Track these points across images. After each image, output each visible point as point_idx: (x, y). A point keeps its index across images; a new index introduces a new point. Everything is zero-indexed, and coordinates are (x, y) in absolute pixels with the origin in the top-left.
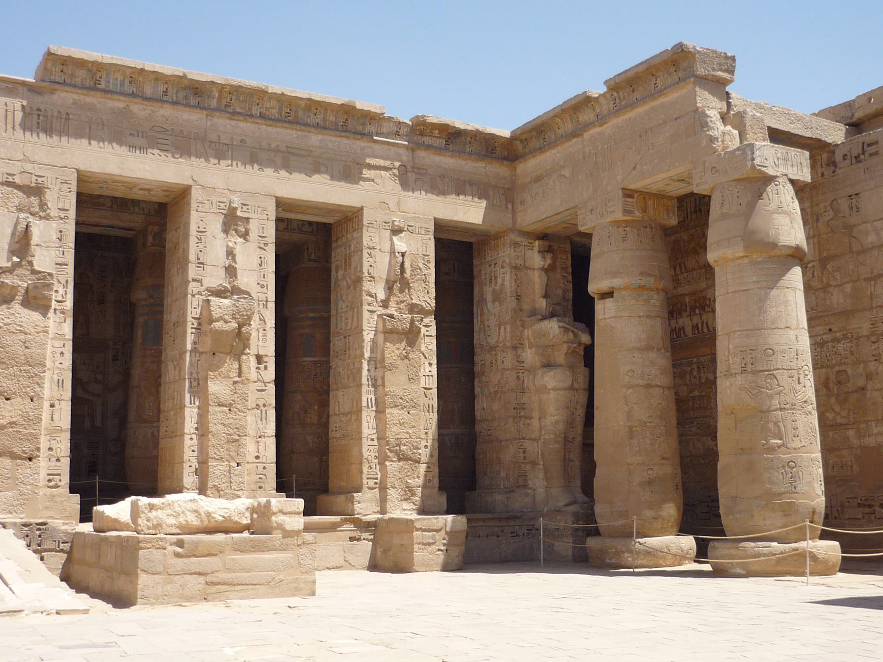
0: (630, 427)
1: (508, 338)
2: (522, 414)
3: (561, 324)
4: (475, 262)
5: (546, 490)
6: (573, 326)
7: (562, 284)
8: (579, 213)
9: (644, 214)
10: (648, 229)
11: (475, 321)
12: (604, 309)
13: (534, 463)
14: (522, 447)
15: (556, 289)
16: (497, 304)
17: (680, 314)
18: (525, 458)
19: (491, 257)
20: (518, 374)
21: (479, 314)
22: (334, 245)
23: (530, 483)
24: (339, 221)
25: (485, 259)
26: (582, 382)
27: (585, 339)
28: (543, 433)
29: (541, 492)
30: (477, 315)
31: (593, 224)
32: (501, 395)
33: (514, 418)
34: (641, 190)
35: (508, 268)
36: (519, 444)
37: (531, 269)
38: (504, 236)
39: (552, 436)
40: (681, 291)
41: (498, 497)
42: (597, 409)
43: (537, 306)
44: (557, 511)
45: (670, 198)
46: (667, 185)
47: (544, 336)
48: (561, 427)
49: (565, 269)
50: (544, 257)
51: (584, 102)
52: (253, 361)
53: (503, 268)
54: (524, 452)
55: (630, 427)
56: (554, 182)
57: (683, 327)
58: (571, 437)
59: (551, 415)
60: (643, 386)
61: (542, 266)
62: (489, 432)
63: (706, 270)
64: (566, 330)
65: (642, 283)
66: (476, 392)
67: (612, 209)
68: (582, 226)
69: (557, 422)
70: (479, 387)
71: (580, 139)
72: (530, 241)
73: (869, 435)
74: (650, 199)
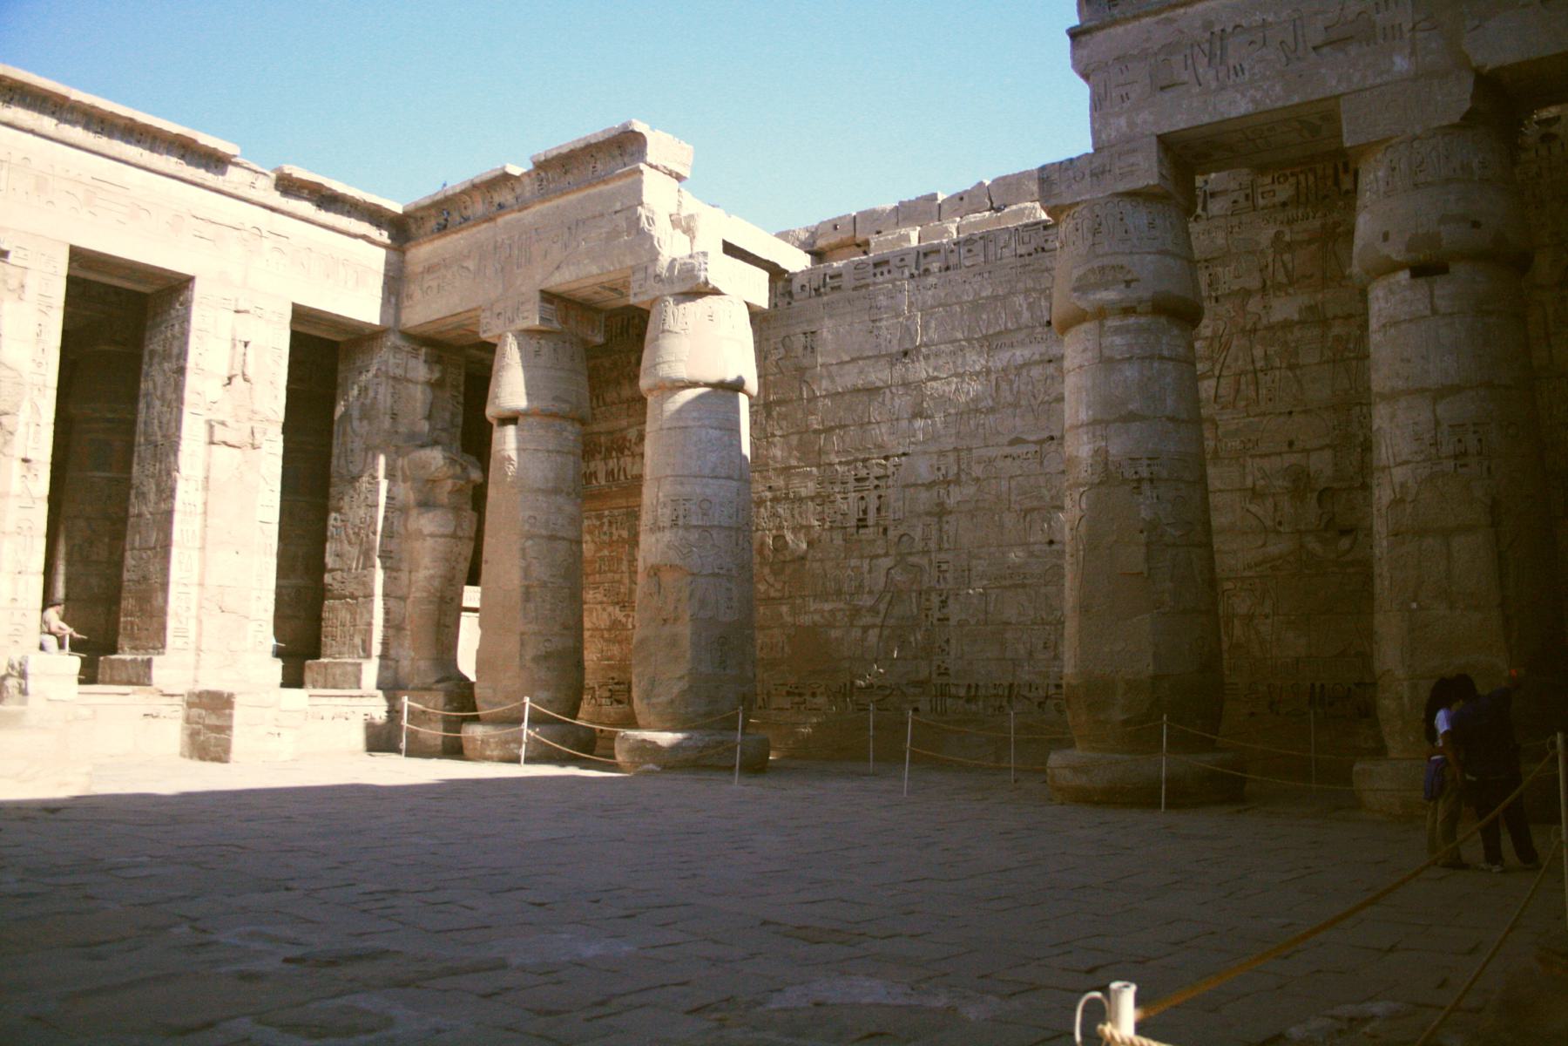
0: (527, 587)
3: (447, 454)
4: (341, 367)
8: (483, 315)
10: (567, 345)
11: (335, 442)
16: (365, 423)
17: (593, 456)
22: (149, 323)
24: (158, 292)
25: (354, 364)
26: (468, 529)
27: (476, 475)
34: (565, 295)
37: (412, 381)
39: (425, 594)
40: (596, 428)
45: (598, 311)
46: (596, 293)
48: (437, 583)
50: (431, 370)
51: (505, 179)
52: (17, 466)
57: (595, 472)
64: (452, 462)
65: (555, 409)
66: (329, 534)
67: (526, 314)
68: (485, 332)
69: (432, 577)
71: (491, 224)
73: (805, 613)
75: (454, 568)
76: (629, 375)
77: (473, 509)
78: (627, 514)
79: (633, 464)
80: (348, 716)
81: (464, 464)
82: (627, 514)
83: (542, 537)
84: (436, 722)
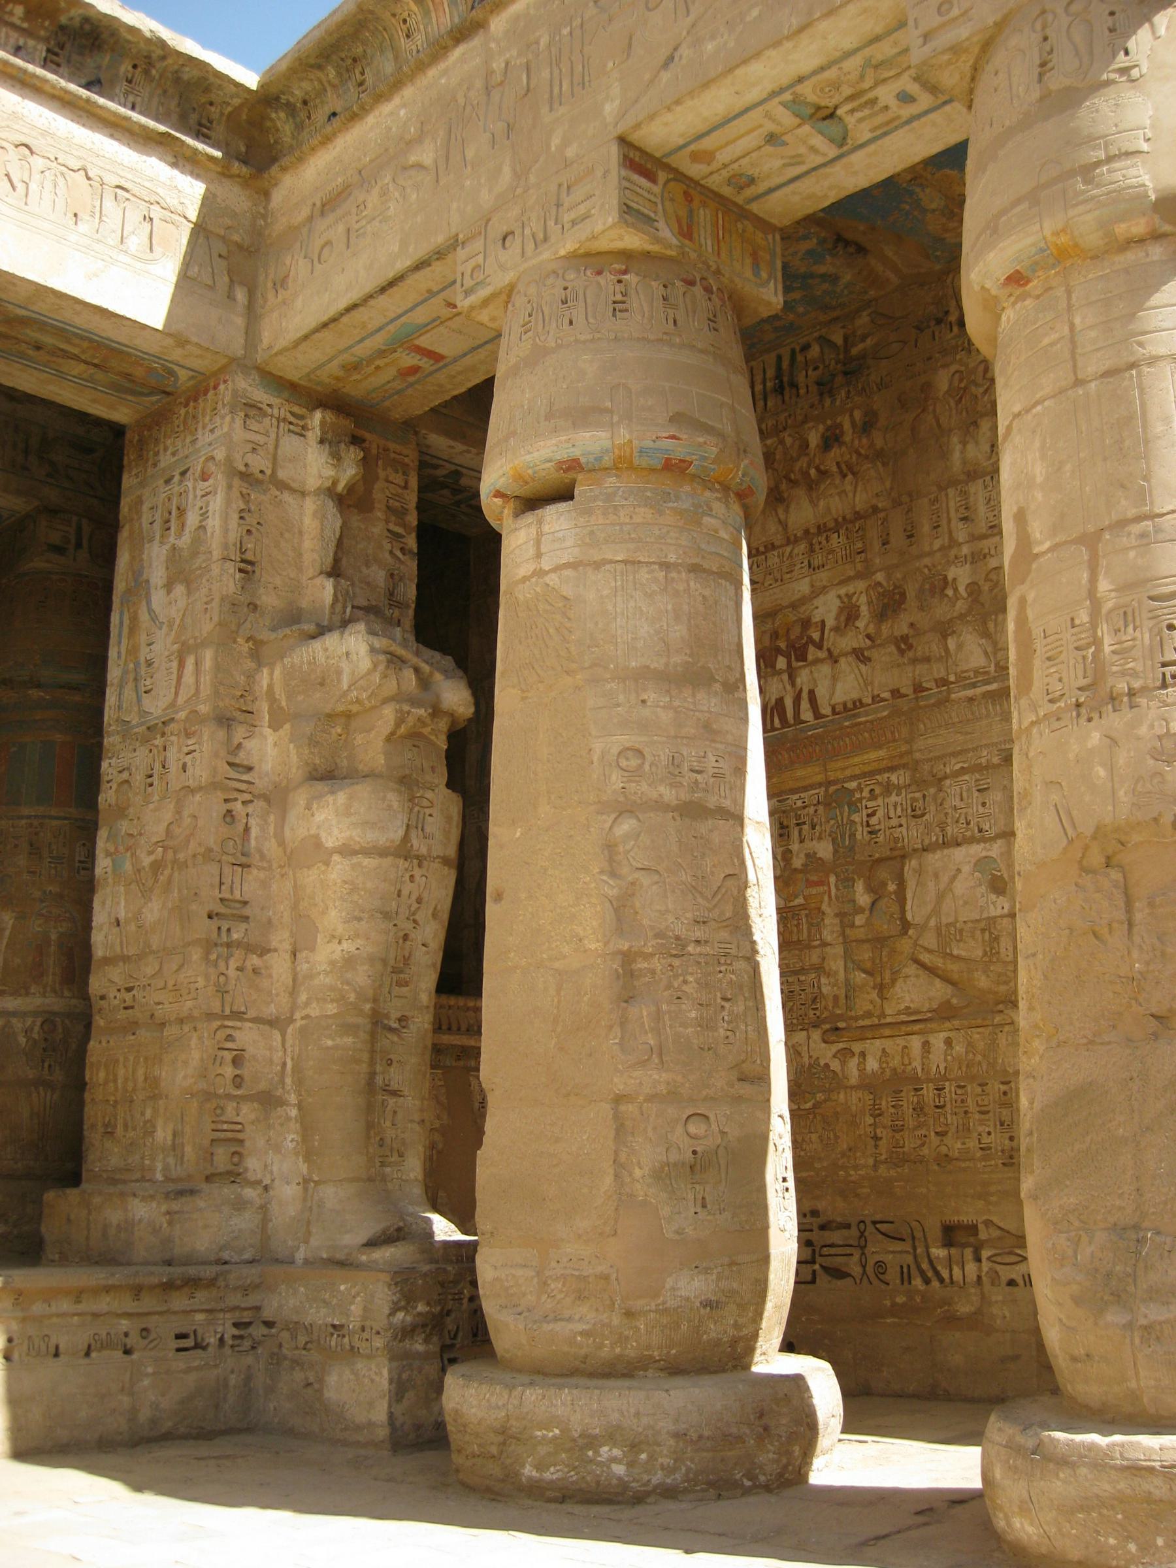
0: (628, 958)
1: (206, 689)
2: (235, 936)
3: (378, 643)
4: (128, 481)
5: (306, 1190)
6: (417, 654)
7: (387, 555)
9: (687, 242)
10: (698, 290)
11: (112, 653)
12: (538, 543)
13: (268, 1101)
14: (229, 1045)
15: (367, 565)
16: (179, 590)
18: (238, 1081)
19: (174, 454)
20: (229, 806)
21: (125, 630)
23: (253, 1165)
28: (303, 997)
29: (288, 1193)
30: (120, 635)
31: (509, 277)
32: (171, 876)
33: (209, 945)
35: (220, 476)
36: (221, 1035)
37: (293, 490)
38: (215, 388)
39: (331, 1009)
41: (143, 1211)
42: (499, 897)
43: (304, 604)
44: (342, 1264)
47: (322, 684)
48: (362, 977)
49: (399, 514)
50: (337, 457)
53: (204, 480)
54: (236, 1062)
55: (628, 958)
56: (384, 193)
58: (395, 1015)
59: (333, 937)
60: (674, 809)
61: (328, 484)
62: (128, 997)
63: (811, 545)
64: (395, 661)
65: (677, 451)
66: (98, 871)
67: (582, 209)
69: (349, 962)
70: (108, 854)
71: (476, 42)
72: (296, 409)
74: (704, 205)
75: (406, 937)
76: (806, 474)
77: (452, 784)
78: (827, 803)
79: (834, 679)
80: (129, 1342)
81: (426, 668)
82: (827, 803)
83: (660, 806)
84: (369, 1357)
